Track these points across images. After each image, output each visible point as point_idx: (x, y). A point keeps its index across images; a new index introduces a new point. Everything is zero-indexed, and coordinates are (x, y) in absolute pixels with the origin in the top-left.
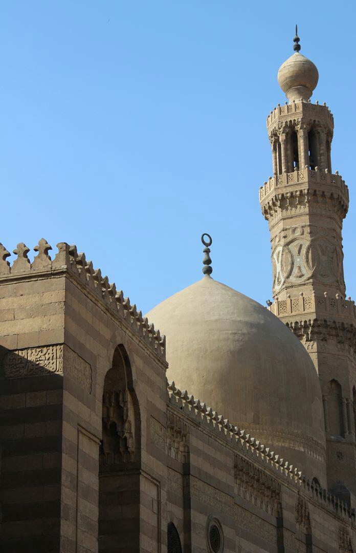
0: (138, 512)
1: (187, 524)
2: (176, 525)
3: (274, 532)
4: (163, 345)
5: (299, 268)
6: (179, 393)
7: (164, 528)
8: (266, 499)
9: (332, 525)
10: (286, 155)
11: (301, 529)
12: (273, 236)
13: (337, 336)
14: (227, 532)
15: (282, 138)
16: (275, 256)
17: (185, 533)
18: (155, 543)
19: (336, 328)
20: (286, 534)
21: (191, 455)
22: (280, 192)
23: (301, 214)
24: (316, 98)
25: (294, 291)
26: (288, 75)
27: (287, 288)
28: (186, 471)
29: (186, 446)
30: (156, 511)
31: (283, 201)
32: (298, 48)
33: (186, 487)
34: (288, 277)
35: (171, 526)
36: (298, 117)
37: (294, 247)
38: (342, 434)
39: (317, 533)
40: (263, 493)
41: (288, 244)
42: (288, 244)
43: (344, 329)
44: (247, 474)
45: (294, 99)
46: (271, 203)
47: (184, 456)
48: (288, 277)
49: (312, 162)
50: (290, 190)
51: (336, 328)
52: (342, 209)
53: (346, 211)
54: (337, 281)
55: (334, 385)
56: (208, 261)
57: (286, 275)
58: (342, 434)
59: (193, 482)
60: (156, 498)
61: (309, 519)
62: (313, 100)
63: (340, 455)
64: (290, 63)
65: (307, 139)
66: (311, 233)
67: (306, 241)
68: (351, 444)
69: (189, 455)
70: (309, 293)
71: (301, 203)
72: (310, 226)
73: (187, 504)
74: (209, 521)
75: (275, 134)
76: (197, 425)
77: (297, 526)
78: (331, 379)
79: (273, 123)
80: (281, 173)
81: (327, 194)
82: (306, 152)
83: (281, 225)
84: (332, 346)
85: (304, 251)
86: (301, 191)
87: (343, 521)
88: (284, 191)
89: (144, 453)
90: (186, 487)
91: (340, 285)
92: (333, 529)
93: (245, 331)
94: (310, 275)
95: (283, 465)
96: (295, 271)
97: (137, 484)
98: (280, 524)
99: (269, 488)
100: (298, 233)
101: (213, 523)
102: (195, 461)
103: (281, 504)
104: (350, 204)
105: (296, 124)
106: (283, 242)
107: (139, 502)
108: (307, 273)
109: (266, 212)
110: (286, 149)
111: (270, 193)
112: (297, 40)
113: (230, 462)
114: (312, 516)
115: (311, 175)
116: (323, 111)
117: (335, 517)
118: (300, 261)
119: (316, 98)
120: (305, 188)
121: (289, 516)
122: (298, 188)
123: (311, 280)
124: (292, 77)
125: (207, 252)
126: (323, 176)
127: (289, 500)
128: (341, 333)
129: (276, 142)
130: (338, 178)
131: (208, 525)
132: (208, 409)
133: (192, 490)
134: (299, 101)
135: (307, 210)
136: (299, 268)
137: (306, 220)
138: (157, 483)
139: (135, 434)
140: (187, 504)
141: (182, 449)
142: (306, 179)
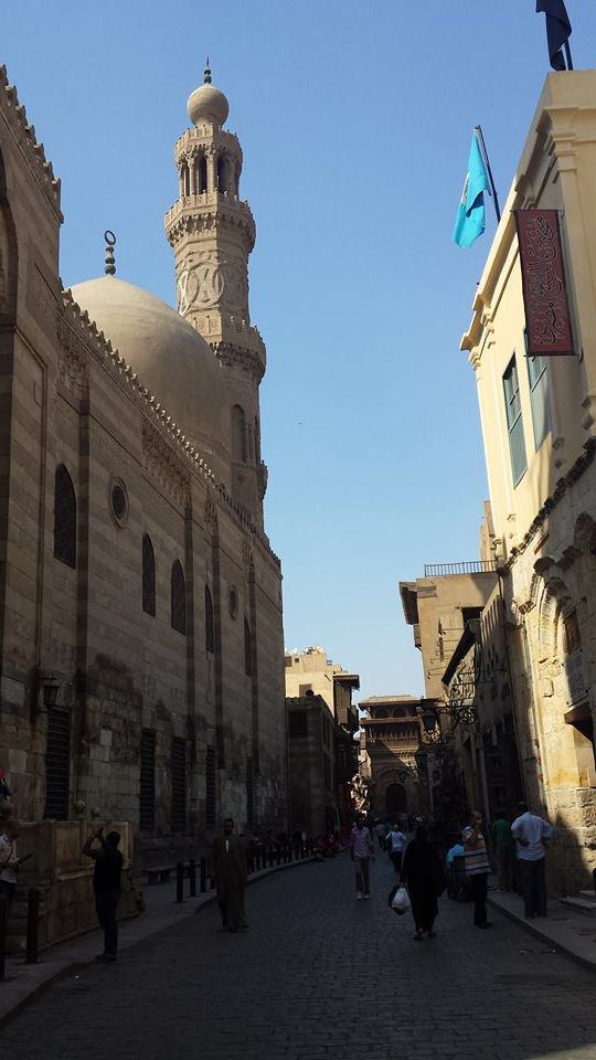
0: (10, 387)
1: (85, 475)
2: (69, 469)
3: (183, 522)
4: (57, 188)
5: (205, 292)
6: (77, 308)
7: (51, 468)
8: (175, 485)
9: (237, 535)
10: (195, 180)
11: (208, 528)
12: (178, 262)
13: (242, 362)
14: (133, 501)
15: (191, 162)
16: (180, 282)
17: (81, 484)
18: (36, 445)
19: (241, 354)
20: (194, 527)
21: (92, 392)
22: (188, 213)
23: (208, 239)
24: (228, 127)
25: (200, 316)
26: (199, 102)
27: (192, 312)
28: (84, 410)
29: (86, 379)
30: (39, 401)
31: (190, 224)
32: (208, 80)
33: (84, 429)
34: (193, 301)
35: (62, 472)
36: (209, 142)
37: (199, 272)
38: (244, 459)
39: (224, 539)
40: (172, 476)
41: (194, 268)
42: (194, 268)
43: (249, 356)
44: (157, 447)
45: (205, 130)
46: (177, 227)
47: (82, 391)
48: (193, 301)
49: (221, 189)
50: (197, 212)
51: (241, 354)
52: (249, 243)
53: (252, 245)
54: (243, 310)
55: (237, 410)
56: (111, 261)
57: (191, 299)
58: (244, 459)
59: (93, 425)
60: (39, 383)
61: (216, 521)
62: (225, 128)
63: (241, 479)
64: (201, 92)
65: (219, 165)
66: (218, 258)
67: (214, 265)
68: (252, 468)
69: (88, 393)
70: (216, 317)
71: (208, 227)
72: (217, 251)
73: (84, 447)
74: (112, 477)
75: (184, 161)
76: (101, 360)
77: (205, 526)
78: (234, 404)
79: (182, 148)
80: (188, 195)
81: (237, 222)
82: (215, 178)
83: (188, 249)
84: (237, 371)
85: (210, 275)
86: (210, 214)
87: (246, 533)
88: (192, 213)
89: (21, 304)
90: (84, 429)
91: (245, 314)
92: (238, 539)
93: (153, 320)
94: (216, 300)
95: (193, 455)
96: (201, 296)
97: (11, 346)
98: (188, 516)
99: (179, 473)
100: (205, 257)
101: (115, 484)
102: (94, 399)
103: (190, 494)
104: (257, 239)
105: (205, 150)
106: (188, 267)
107: (11, 373)
108: (214, 296)
109: (171, 238)
110: (195, 175)
111: (177, 213)
112: (208, 72)
113: (138, 424)
114: (220, 519)
115: (221, 199)
116: (233, 139)
117: (240, 527)
118: (206, 285)
119: (228, 127)
120: (214, 210)
121: (199, 512)
122: (206, 211)
123: (217, 305)
124: (202, 104)
125: (111, 250)
126: (232, 203)
127: (199, 495)
128: (246, 360)
129: (185, 168)
130: (244, 207)
131: (110, 482)
132: (114, 350)
133: (91, 435)
134: (210, 128)
135: (215, 234)
136: (205, 292)
137: (213, 245)
138: (43, 365)
139: (9, 275)
140: (84, 447)
141: (79, 381)
142: (215, 202)
